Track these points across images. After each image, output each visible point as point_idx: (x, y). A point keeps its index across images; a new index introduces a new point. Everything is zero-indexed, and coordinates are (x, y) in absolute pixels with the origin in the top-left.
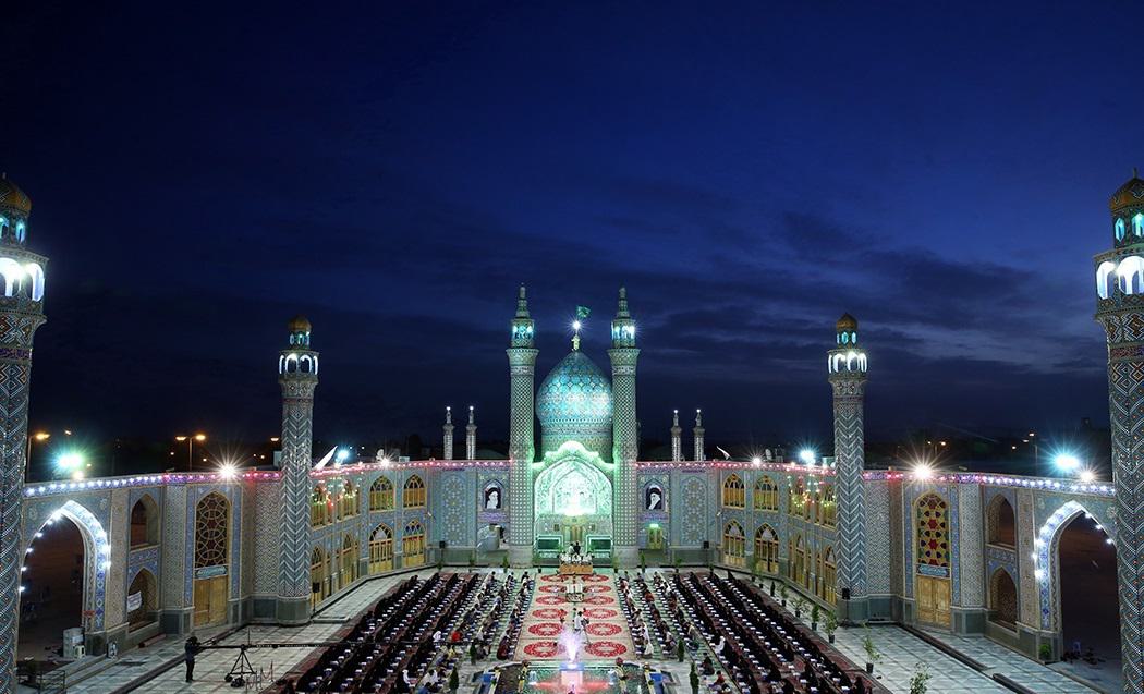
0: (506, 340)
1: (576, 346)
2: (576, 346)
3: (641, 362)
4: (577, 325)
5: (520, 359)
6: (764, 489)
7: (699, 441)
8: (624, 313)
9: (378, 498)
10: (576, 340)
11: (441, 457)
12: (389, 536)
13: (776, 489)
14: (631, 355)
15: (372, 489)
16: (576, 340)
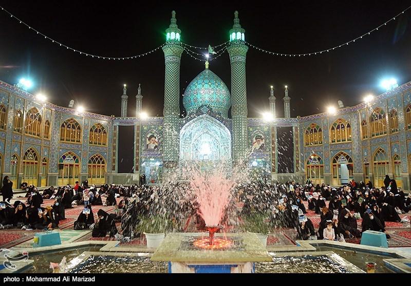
0: (163, 41)
1: (207, 67)
2: (207, 67)
3: (249, 56)
4: (207, 56)
5: (171, 57)
6: (338, 127)
7: (287, 106)
8: (237, 25)
9: (68, 132)
10: (207, 64)
11: (118, 114)
12: (77, 161)
13: (349, 126)
14: (244, 50)
15: (63, 126)
16: (207, 64)
